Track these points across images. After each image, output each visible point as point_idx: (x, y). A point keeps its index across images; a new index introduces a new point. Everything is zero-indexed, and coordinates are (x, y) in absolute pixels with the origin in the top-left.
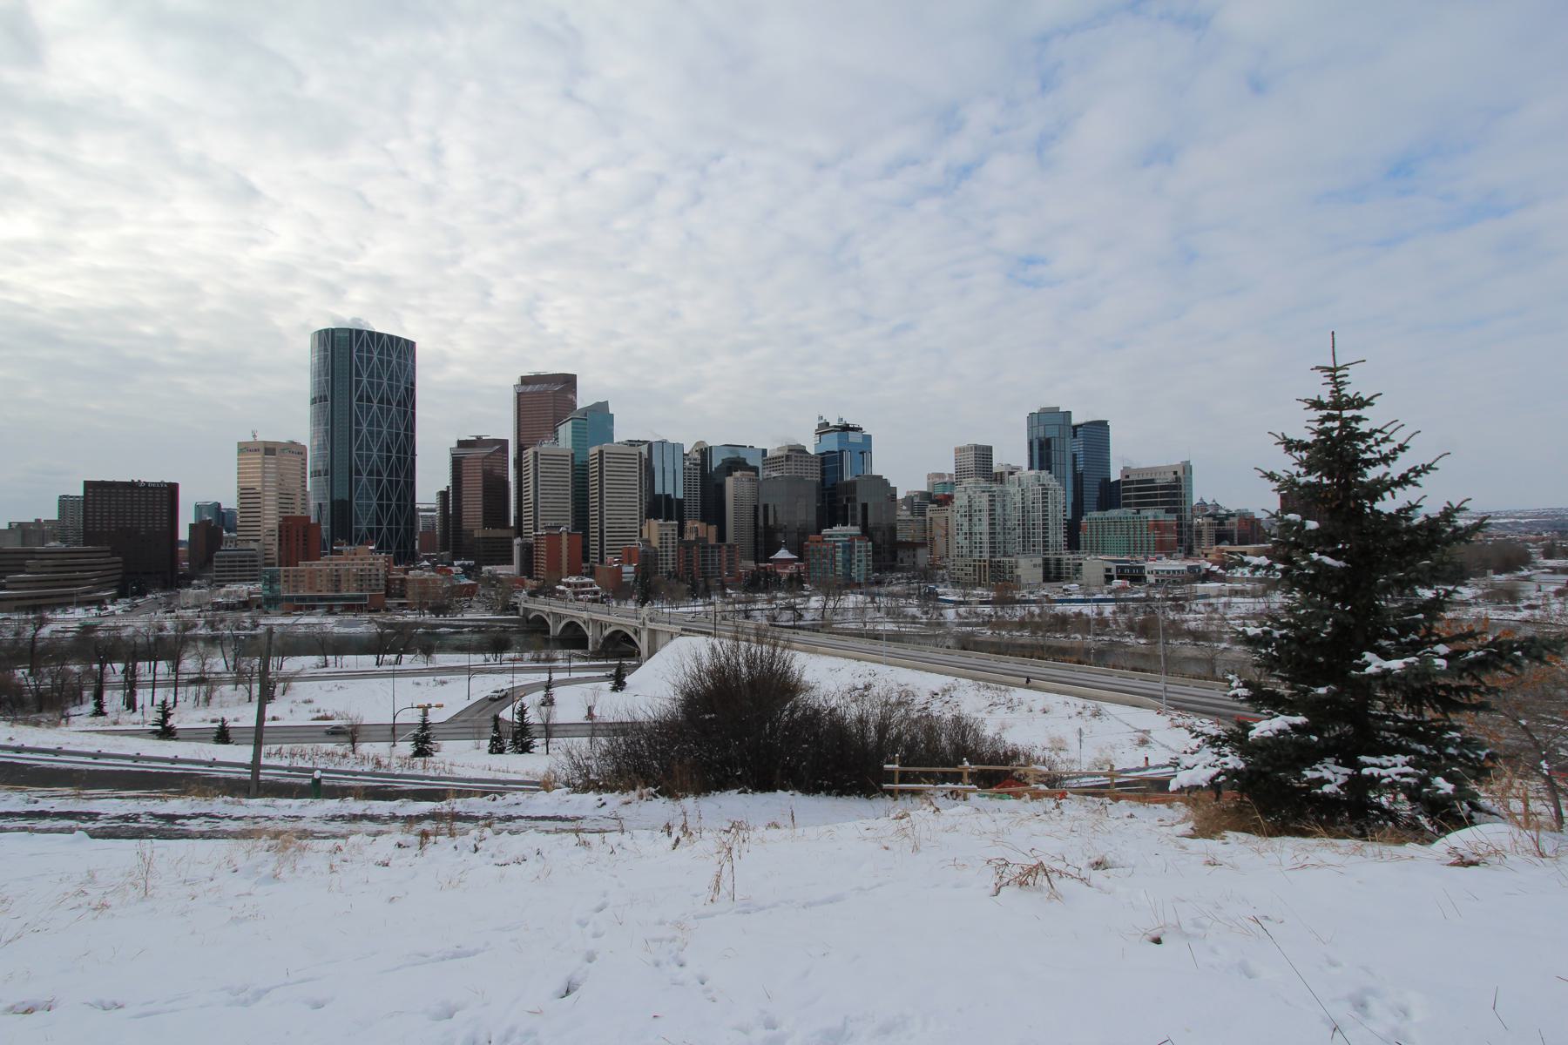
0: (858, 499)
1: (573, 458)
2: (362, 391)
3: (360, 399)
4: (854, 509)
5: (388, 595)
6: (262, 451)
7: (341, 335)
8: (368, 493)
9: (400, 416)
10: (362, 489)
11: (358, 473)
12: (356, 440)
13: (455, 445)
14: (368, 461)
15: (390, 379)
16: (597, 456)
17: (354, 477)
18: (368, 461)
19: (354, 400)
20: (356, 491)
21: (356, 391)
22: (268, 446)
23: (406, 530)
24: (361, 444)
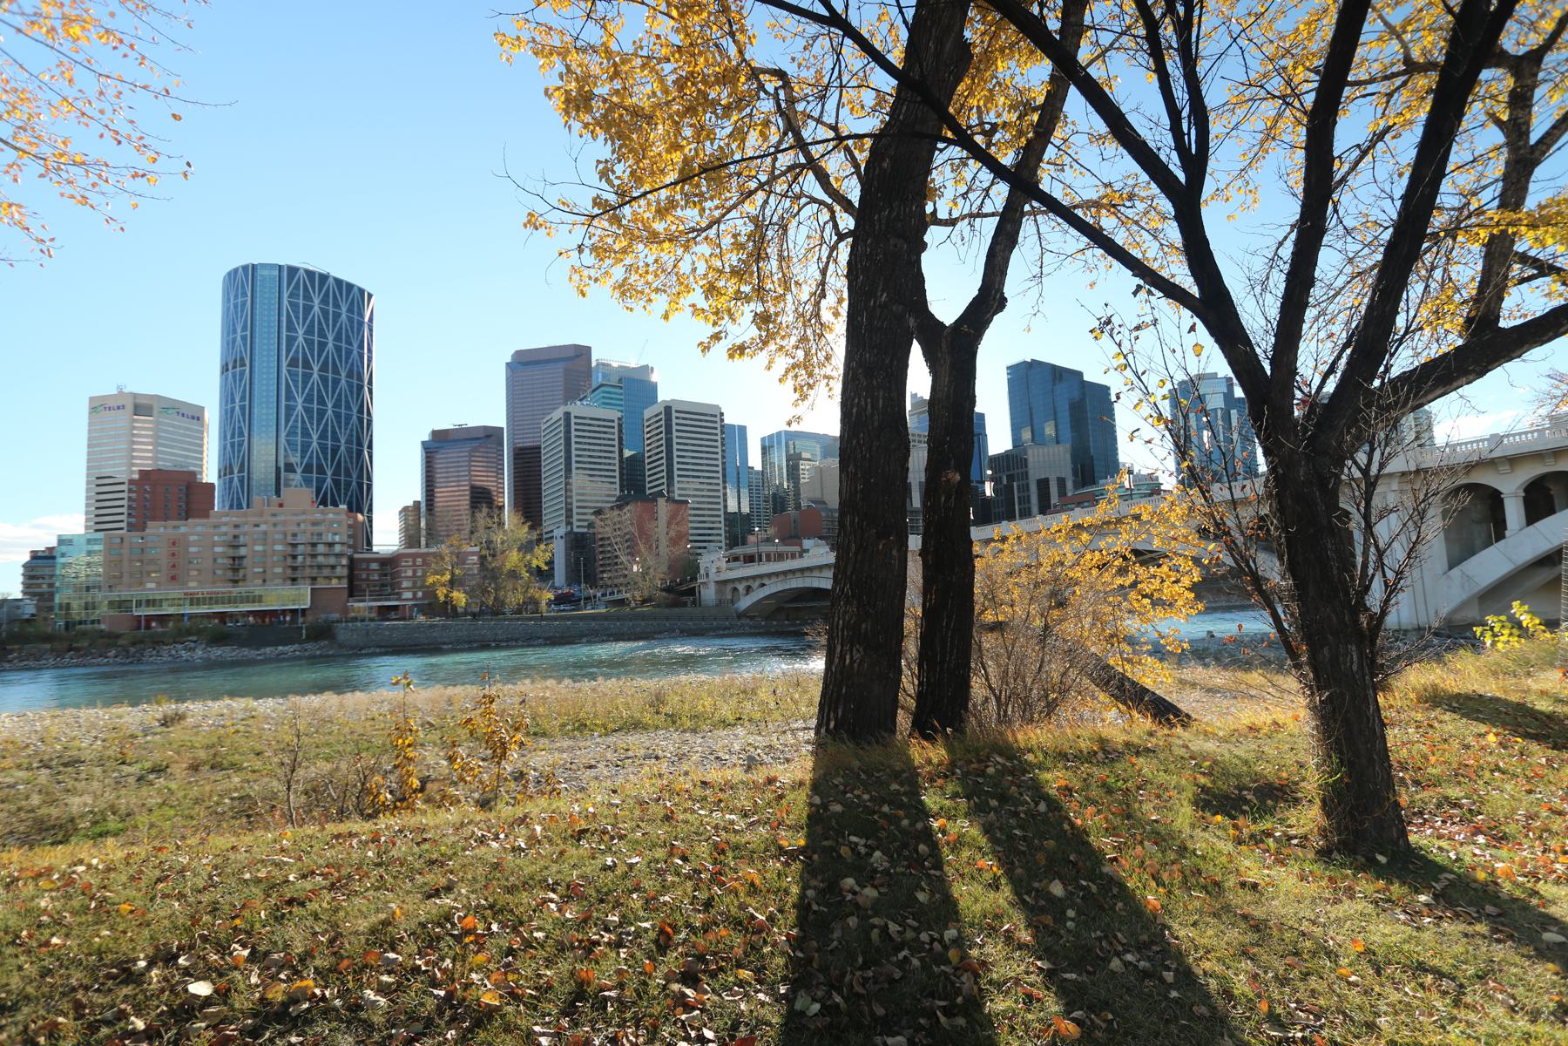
0: (1031, 472)
1: (620, 426)
2: (297, 351)
3: (293, 363)
4: (1025, 488)
5: (353, 591)
6: (130, 408)
7: (266, 273)
9: (352, 393)
12: (287, 421)
15: (338, 338)
16: (662, 416)
19: (284, 364)
21: (288, 351)
22: (139, 401)
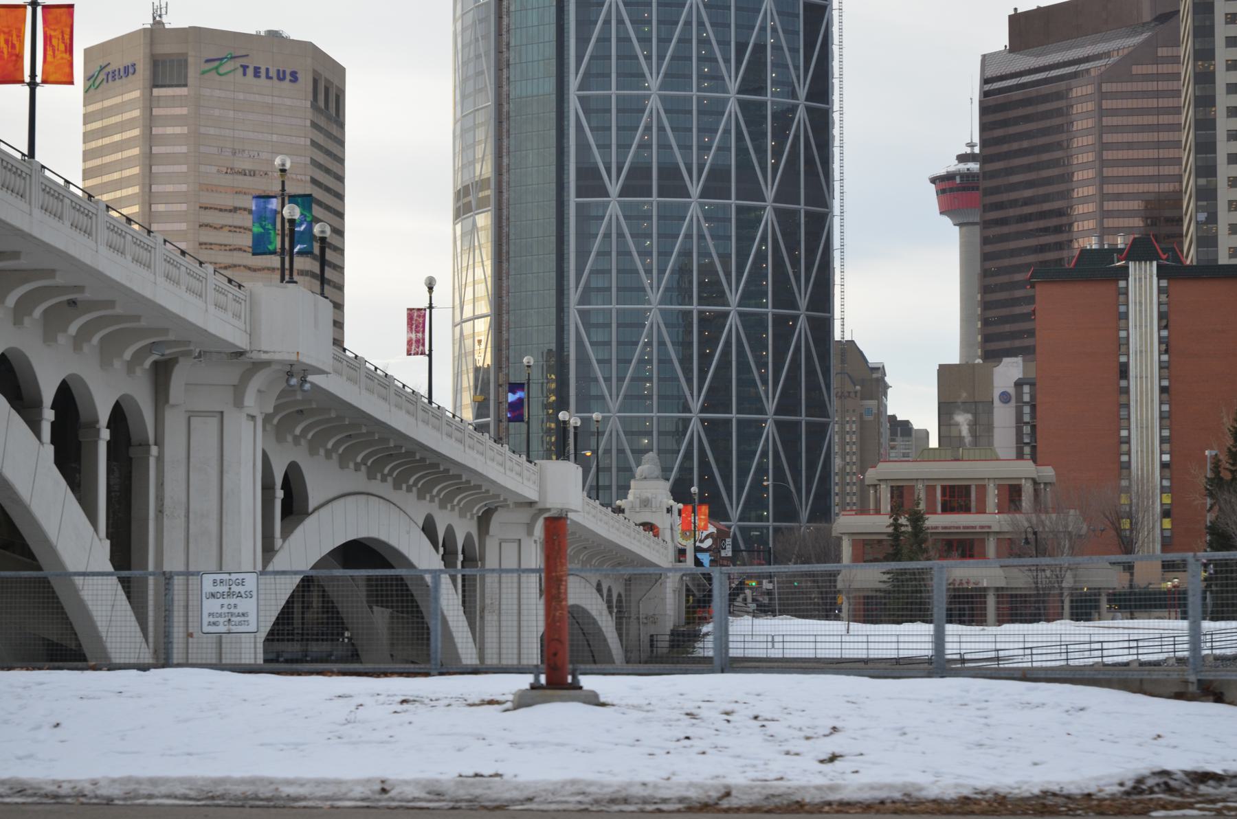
6: (143, 70)
8: (627, 271)
10: (604, 254)
11: (591, 183)
12: (582, 41)
13: (1000, 40)
14: (627, 129)
17: (573, 200)
18: (627, 129)
20: (582, 255)
23: (787, 431)
24: (602, 56)
